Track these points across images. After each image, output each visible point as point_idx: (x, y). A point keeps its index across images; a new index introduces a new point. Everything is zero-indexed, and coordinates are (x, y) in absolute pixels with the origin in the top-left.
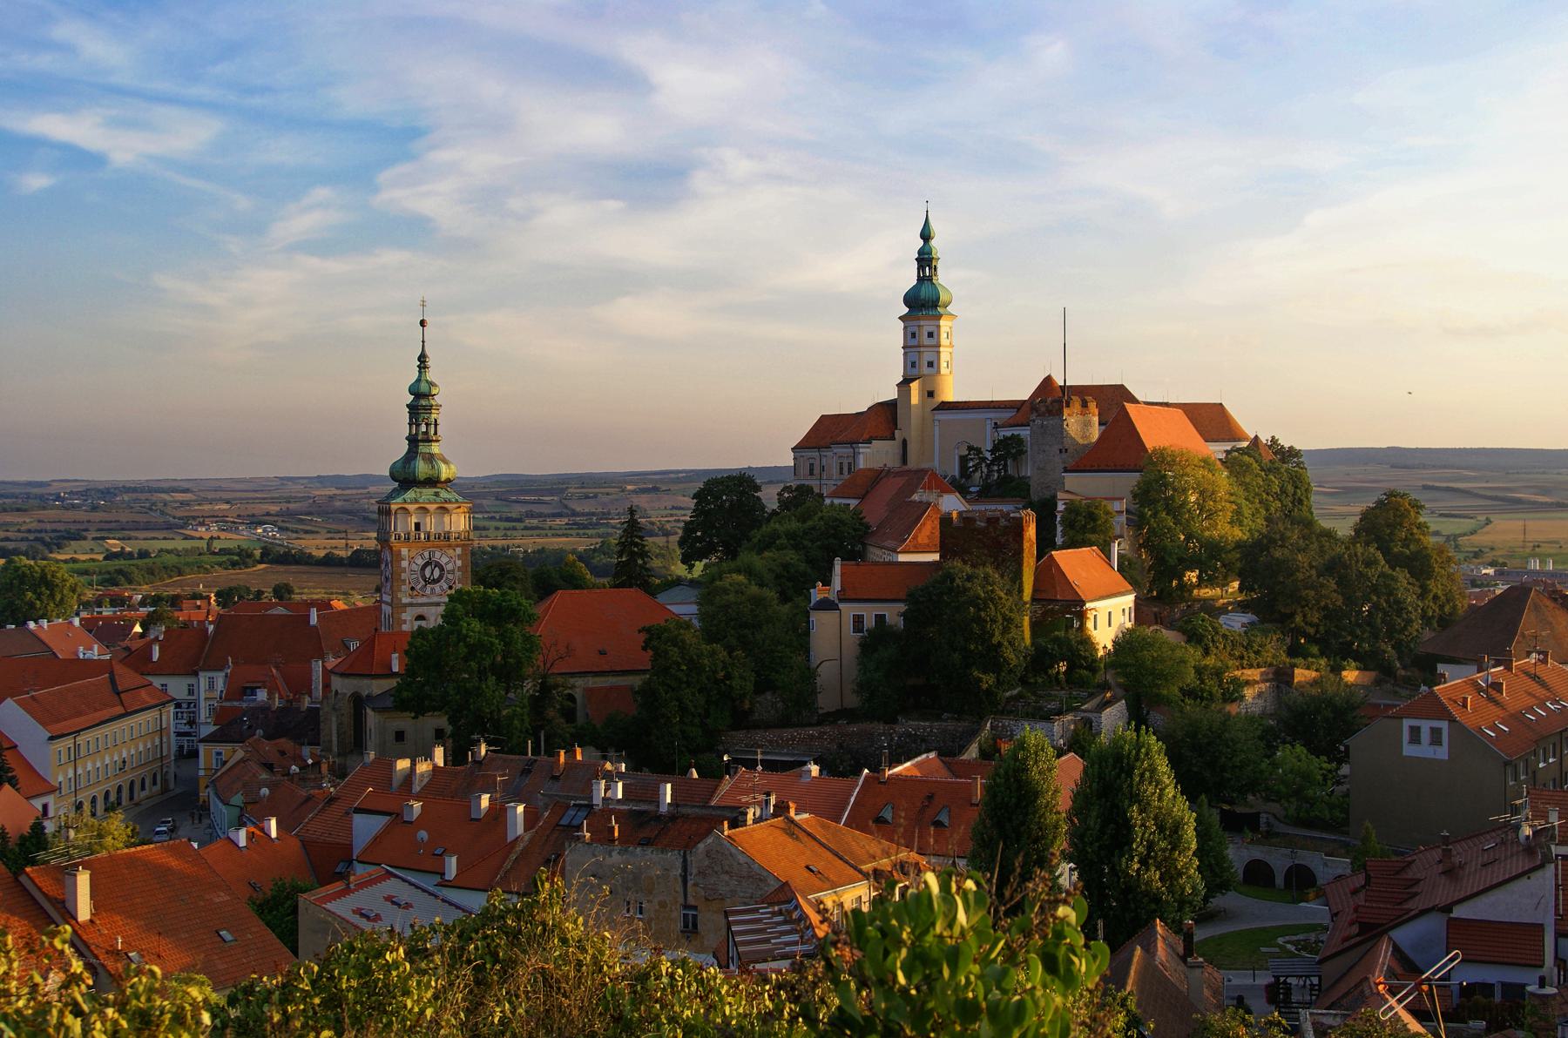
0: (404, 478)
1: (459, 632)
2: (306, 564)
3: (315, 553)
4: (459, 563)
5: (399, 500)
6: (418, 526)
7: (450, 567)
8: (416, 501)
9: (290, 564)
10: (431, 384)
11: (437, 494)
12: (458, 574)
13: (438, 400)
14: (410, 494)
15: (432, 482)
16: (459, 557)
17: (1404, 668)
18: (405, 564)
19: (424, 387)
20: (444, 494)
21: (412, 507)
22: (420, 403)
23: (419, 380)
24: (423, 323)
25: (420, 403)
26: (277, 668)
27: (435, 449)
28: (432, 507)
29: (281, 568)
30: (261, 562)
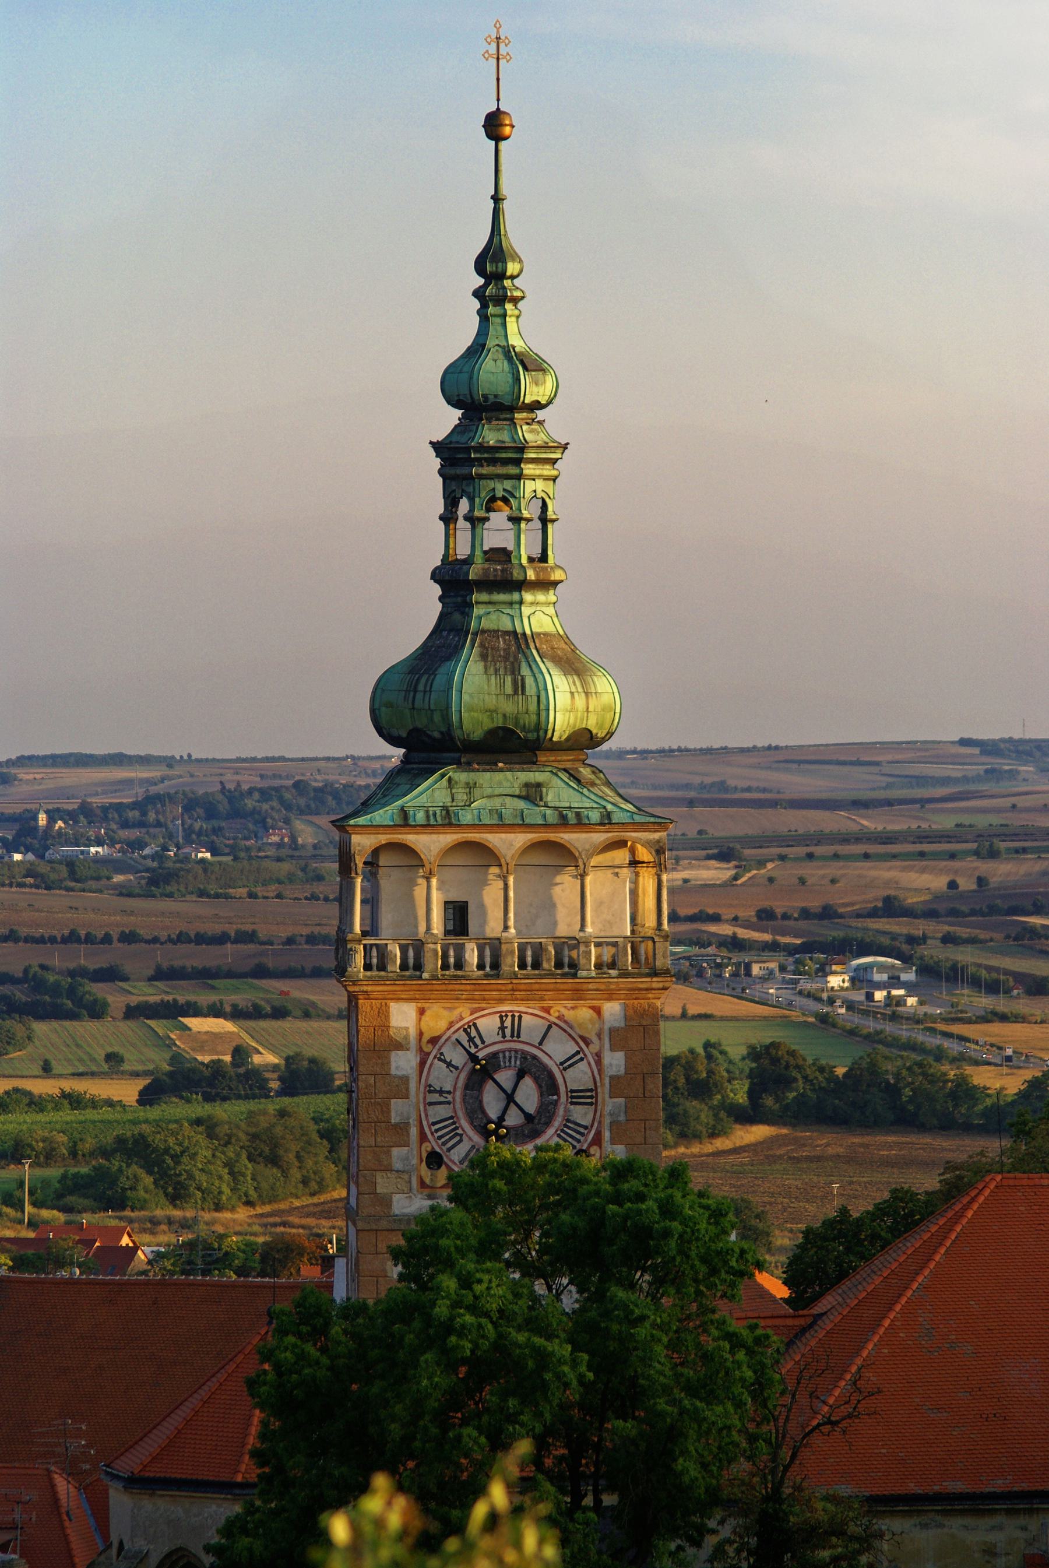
0: (419, 723)
1: (428, 1320)
2: (947, 1125)
3: (984, 1078)
4: (615, 1061)
5: (382, 815)
6: (459, 917)
7: (579, 1076)
8: (448, 820)
9: (871, 1123)
10: (527, 363)
11: (532, 793)
12: (610, 1104)
13: (555, 423)
14: (430, 794)
15: (518, 743)
16: (618, 1038)
17: (629, 1208)
18: (404, 1063)
19: (492, 373)
20: (560, 793)
21: (430, 844)
22: (484, 440)
23: (477, 350)
24: (494, 126)
25: (484, 440)
26: (72, 1472)
27: (538, 615)
28: (509, 844)
29: (830, 1142)
30: (747, 1116)
